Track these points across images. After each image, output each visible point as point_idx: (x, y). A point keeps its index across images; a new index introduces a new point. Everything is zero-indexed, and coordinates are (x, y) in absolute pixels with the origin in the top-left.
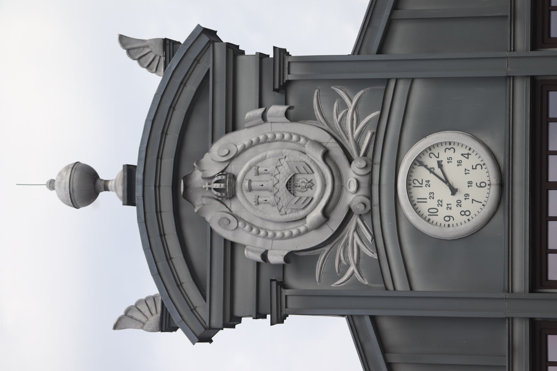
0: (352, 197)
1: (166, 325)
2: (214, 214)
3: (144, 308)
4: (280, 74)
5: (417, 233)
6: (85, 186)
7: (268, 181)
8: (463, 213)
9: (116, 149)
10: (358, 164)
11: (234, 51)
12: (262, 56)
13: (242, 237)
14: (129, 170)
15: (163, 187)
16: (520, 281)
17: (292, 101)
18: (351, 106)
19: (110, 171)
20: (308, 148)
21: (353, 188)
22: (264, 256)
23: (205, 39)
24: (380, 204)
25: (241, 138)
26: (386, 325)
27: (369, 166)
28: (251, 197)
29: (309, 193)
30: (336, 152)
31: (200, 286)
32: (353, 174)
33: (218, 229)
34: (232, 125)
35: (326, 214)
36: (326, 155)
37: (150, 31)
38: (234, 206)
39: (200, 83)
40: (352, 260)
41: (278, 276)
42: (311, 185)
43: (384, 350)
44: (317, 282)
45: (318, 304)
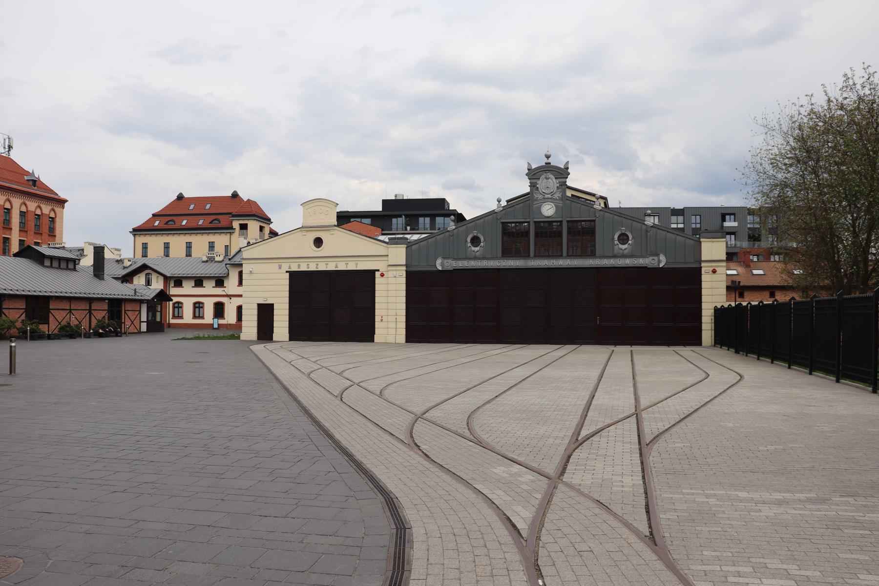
2: (543, 176)
6: (548, 157)
7: (549, 184)
9: (553, 162)
15: (548, 168)
19: (550, 160)
24: (546, 200)
31: (534, 174)
32: (549, 196)
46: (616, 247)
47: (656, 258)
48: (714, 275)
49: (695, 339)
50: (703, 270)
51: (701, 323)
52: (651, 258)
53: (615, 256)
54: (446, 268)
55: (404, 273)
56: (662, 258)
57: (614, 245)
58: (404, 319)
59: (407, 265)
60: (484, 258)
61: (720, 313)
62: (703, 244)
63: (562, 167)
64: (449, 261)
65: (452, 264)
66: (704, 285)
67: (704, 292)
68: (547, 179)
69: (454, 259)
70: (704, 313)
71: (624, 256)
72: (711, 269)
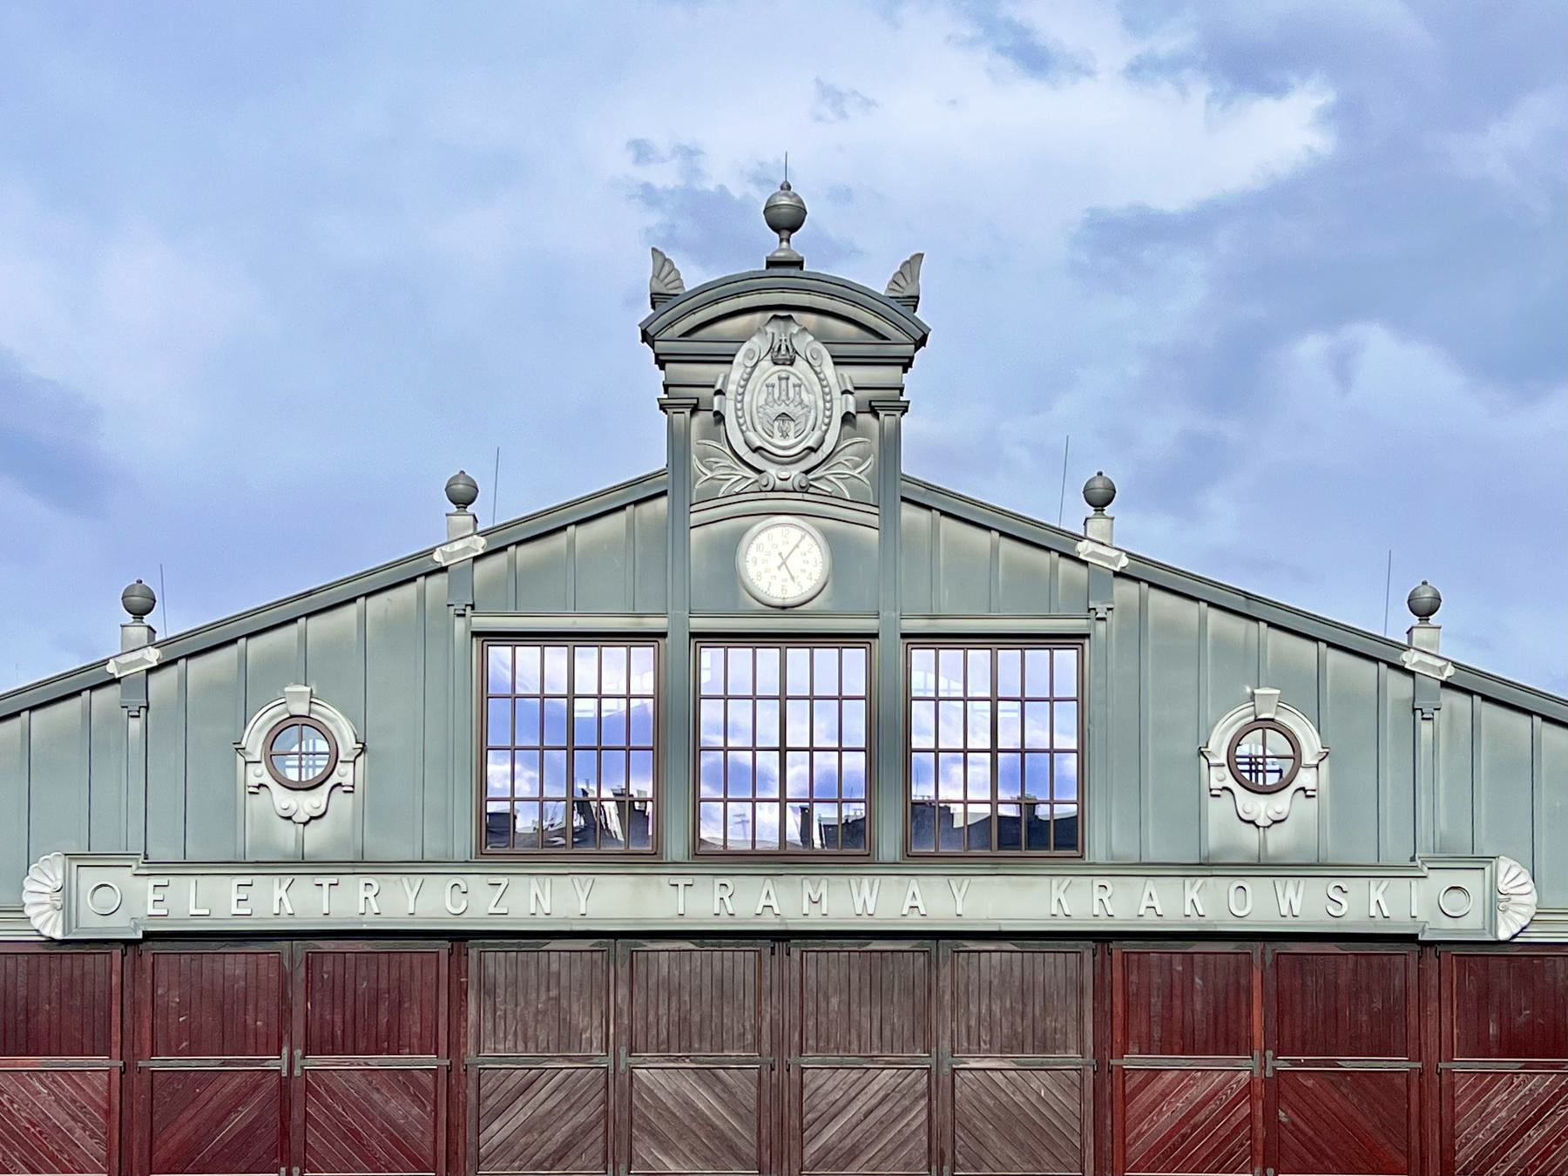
0: (773, 472)
2: (758, 344)
3: (677, 283)
5: (740, 534)
6: (786, 222)
8: (759, 575)
11: (906, 366)
12: (901, 390)
13: (736, 372)
14: (799, 264)
16: (698, 624)
17: (860, 417)
18: (855, 473)
20: (817, 434)
21: (784, 475)
22: (719, 392)
23: (919, 335)
26: (662, 503)
28: (774, 380)
29: (777, 434)
30: (814, 459)
33: (746, 346)
34: (839, 361)
35: (756, 450)
36: (812, 450)
37: (927, 284)
38: (766, 363)
42: (785, 435)
45: (678, 444)
46: (1218, 810)
47: (1472, 881)
53: (1207, 866)
54: (92, 924)
56: (1511, 876)
57: (1201, 795)
60: (361, 864)
64: (121, 878)
65: (127, 903)
68: (784, 357)
69: (152, 866)
71: (1264, 866)
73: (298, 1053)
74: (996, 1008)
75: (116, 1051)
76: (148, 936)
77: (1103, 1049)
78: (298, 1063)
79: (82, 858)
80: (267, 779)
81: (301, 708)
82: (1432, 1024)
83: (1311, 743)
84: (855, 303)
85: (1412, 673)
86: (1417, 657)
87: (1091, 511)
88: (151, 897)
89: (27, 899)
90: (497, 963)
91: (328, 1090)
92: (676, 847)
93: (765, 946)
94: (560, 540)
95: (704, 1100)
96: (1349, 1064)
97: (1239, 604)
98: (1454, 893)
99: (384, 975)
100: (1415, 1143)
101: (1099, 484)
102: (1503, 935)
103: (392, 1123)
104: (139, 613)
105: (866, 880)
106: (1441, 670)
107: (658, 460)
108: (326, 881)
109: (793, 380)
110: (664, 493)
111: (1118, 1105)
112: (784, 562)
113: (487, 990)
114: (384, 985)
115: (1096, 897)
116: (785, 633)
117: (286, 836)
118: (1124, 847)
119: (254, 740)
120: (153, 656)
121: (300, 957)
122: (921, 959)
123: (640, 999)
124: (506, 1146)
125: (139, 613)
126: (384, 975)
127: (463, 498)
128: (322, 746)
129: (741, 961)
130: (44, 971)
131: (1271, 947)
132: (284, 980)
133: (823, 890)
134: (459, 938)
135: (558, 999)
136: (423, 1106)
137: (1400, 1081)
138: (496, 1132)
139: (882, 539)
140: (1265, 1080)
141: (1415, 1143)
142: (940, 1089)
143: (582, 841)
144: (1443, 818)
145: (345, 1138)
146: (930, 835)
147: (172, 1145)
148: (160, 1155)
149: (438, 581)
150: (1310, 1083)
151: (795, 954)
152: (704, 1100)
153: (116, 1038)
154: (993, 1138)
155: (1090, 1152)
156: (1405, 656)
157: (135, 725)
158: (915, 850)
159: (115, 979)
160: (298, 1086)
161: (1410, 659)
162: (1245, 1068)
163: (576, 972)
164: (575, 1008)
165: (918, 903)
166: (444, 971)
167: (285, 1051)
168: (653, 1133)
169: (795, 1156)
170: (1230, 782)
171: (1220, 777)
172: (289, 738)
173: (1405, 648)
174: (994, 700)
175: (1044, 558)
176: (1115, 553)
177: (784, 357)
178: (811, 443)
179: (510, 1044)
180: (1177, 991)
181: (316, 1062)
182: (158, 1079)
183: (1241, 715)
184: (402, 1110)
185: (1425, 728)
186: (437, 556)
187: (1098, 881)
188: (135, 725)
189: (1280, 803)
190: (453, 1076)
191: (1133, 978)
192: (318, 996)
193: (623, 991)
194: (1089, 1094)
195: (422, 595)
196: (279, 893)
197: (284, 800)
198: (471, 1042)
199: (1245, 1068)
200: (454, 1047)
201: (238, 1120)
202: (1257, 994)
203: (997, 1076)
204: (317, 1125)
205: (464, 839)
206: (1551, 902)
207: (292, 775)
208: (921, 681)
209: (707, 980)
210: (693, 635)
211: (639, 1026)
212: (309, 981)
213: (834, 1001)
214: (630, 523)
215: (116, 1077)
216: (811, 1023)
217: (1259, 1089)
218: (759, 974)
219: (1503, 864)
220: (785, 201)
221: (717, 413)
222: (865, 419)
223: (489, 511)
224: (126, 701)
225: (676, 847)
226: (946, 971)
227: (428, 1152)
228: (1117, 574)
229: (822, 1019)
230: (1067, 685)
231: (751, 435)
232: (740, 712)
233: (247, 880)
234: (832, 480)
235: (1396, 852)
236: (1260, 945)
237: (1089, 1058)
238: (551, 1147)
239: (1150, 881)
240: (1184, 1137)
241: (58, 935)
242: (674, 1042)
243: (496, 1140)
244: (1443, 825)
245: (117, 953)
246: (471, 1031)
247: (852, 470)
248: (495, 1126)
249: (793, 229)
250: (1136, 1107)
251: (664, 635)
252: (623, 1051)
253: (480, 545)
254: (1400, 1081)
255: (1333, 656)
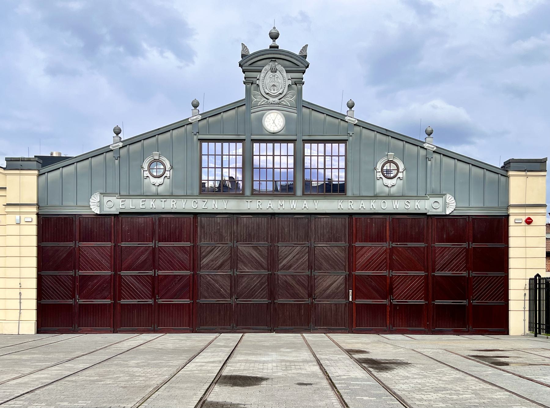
0: (271, 100)
1: (243, 56)
2: (267, 67)
4: (299, 82)
5: (263, 114)
6: (274, 36)
7: (274, 80)
9: (282, 44)
10: (278, 101)
11: (304, 72)
12: (302, 79)
13: (262, 74)
14: (278, 47)
15: (274, 55)
17: (293, 86)
20: (282, 90)
25: (285, 74)
26: (244, 107)
27: (278, 104)
28: (271, 76)
31: (251, 64)
32: (276, 100)
34: (287, 72)
35: (267, 94)
36: (281, 94)
37: (309, 52)
38: (270, 72)
39: (297, 64)
40: (257, 100)
41: (254, 82)
42: (274, 90)
43: (238, 107)
44: (253, 92)
45: (248, 92)
46: (379, 183)
47: (440, 200)
48: (528, 227)
49: (498, 323)
50: (512, 220)
51: (507, 300)
52: (432, 200)
53: (376, 197)
54: (107, 210)
55: (35, 217)
57: (375, 179)
58: (33, 294)
59: (38, 205)
60: (172, 196)
61: (535, 283)
62: (512, 179)
63: (298, 53)
64: (113, 199)
65: (114, 205)
66: (512, 242)
67: (512, 253)
68: (274, 71)
69: (121, 196)
70: (512, 284)
72: (524, 218)
73: (157, 242)
74: (325, 231)
75: (113, 241)
76: (121, 213)
77: (350, 241)
78: (157, 244)
79: (104, 194)
80: (149, 175)
81: (157, 158)
82: (430, 235)
83: (401, 167)
84: (291, 57)
85: (426, 149)
86: (427, 145)
87: (348, 109)
88: (121, 204)
89: (91, 204)
90: (204, 219)
91: (164, 251)
92: (248, 192)
93: (269, 217)
94: (219, 117)
95: (254, 253)
96: (410, 244)
97: (384, 132)
98: (436, 204)
99: (177, 223)
100: (426, 264)
101: (350, 102)
102: (448, 213)
103: (180, 259)
104: (117, 134)
105: (293, 201)
106: (433, 148)
107: (243, 96)
108: (163, 200)
109: (276, 76)
110: (245, 105)
111: (354, 255)
112: (274, 122)
113: (202, 227)
114: (177, 225)
115: (349, 204)
116: (274, 139)
117: (154, 189)
118: (357, 193)
119: (145, 166)
120: (121, 144)
121: (157, 219)
122: (307, 220)
123: (239, 229)
124: (207, 264)
125: (117, 134)
126: (177, 223)
127: (196, 106)
128: (162, 167)
129: (264, 220)
130: (95, 222)
131: (391, 216)
132: (153, 224)
133: (283, 202)
134: (196, 214)
135: (219, 229)
136: (187, 255)
137: (422, 249)
138: (205, 261)
139: (298, 116)
140: (390, 249)
141: (426, 264)
142: (311, 251)
143: (225, 189)
144: (434, 184)
145: (168, 262)
146: (310, 190)
147: (126, 264)
148: (123, 267)
149: (189, 127)
150: (400, 249)
151: (277, 218)
152: (254, 253)
153: (113, 238)
154: (325, 264)
155: (347, 267)
156: (424, 145)
157: (117, 161)
158: (306, 193)
159: (112, 224)
160: (157, 251)
161: (426, 146)
162: (385, 245)
163: (224, 223)
164: (224, 231)
165: (306, 206)
166: (192, 222)
167: (154, 241)
168: (243, 262)
169: (276, 267)
170: (382, 176)
171: (379, 175)
172: (154, 166)
173: (424, 143)
174: (325, 156)
175: (337, 121)
176: (354, 120)
177: (274, 71)
178: (280, 92)
179: (208, 240)
180: (368, 227)
181: (161, 244)
182: (123, 248)
183: (384, 160)
184: (181, 256)
185: (429, 163)
186: (189, 120)
187: (350, 201)
188: (117, 161)
189: (394, 181)
190: (194, 247)
191: (358, 224)
192: (162, 228)
193: (235, 227)
194: (347, 252)
195: (186, 130)
196: (152, 203)
197: (153, 180)
198: (199, 239)
199: (385, 245)
200: (194, 241)
201: (143, 258)
202: (388, 228)
203: (325, 248)
204: (161, 259)
205: (196, 191)
206: (459, 205)
207: (155, 174)
208: (307, 152)
209: (255, 225)
210: (252, 140)
211: (239, 236)
212: (159, 224)
213: (286, 230)
214: (237, 112)
215: (113, 248)
216: (280, 235)
217: (388, 251)
218: (268, 223)
219: (448, 196)
220: (273, 31)
221: (257, 85)
222: (294, 86)
223: (202, 109)
224: (115, 155)
225: (248, 192)
226: (313, 222)
227: (188, 265)
228: (355, 125)
229: (283, 234)
230: (342, 152)
231: (266, 90)
232: (263, 158)
233: (144, 200)
234: (285, 101)
235: (422, 193)
236: (388, 216)
237: (347, 244)
238: (218, 265)
239: (362, 201)
240: (370, 262)
241: (98, 213)
242: (247, 240)
243: (205, 263)
244: (433, 186)
245: (113, 217)
246: (199, 237)
247: (290, 99)
248: (204, 260)
249: (276, 39)
250: (358, 256)
251: (245, 140)
252: (235, 242)
253: (200, 117)
254: (422, 249)
255: (407, 145)
